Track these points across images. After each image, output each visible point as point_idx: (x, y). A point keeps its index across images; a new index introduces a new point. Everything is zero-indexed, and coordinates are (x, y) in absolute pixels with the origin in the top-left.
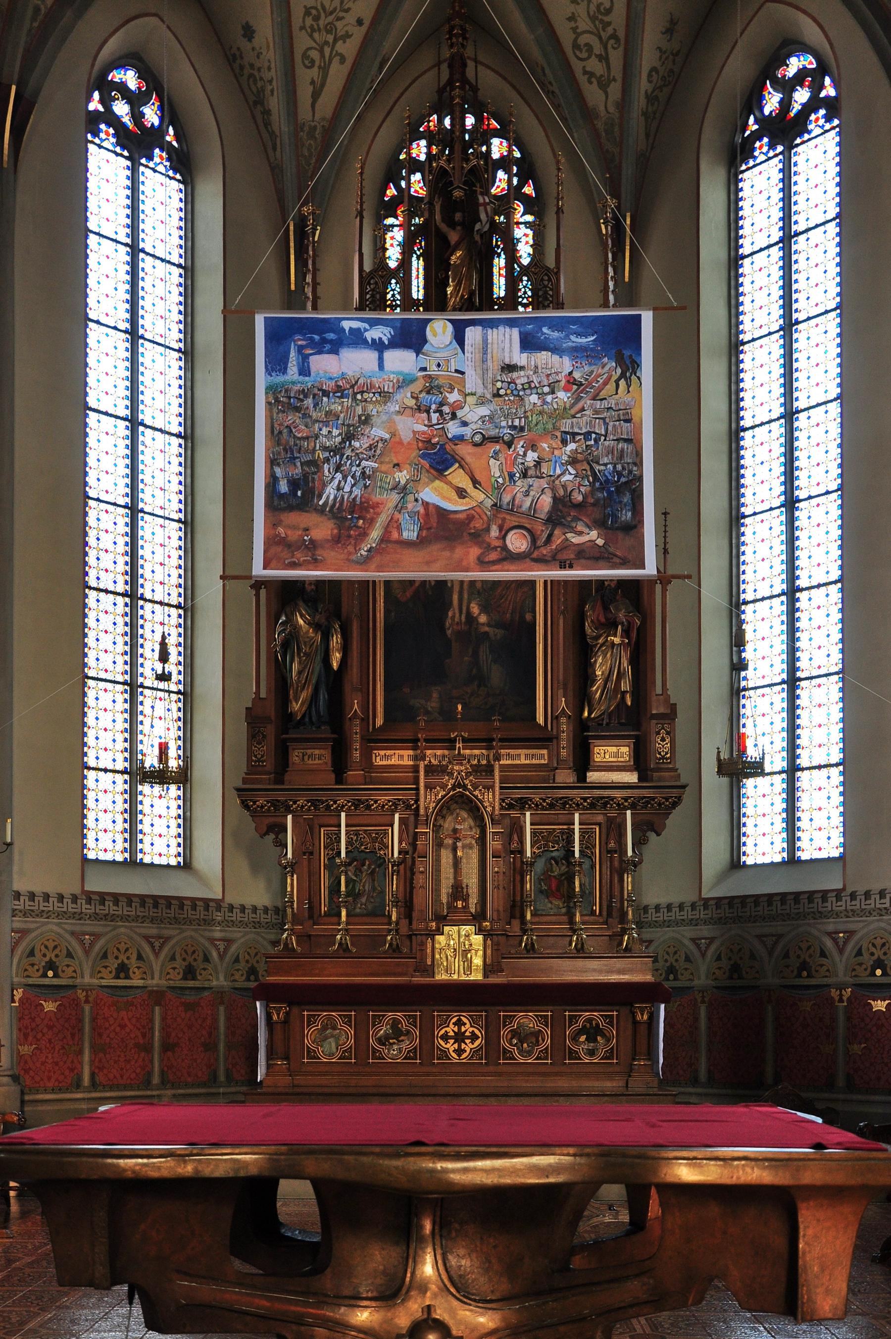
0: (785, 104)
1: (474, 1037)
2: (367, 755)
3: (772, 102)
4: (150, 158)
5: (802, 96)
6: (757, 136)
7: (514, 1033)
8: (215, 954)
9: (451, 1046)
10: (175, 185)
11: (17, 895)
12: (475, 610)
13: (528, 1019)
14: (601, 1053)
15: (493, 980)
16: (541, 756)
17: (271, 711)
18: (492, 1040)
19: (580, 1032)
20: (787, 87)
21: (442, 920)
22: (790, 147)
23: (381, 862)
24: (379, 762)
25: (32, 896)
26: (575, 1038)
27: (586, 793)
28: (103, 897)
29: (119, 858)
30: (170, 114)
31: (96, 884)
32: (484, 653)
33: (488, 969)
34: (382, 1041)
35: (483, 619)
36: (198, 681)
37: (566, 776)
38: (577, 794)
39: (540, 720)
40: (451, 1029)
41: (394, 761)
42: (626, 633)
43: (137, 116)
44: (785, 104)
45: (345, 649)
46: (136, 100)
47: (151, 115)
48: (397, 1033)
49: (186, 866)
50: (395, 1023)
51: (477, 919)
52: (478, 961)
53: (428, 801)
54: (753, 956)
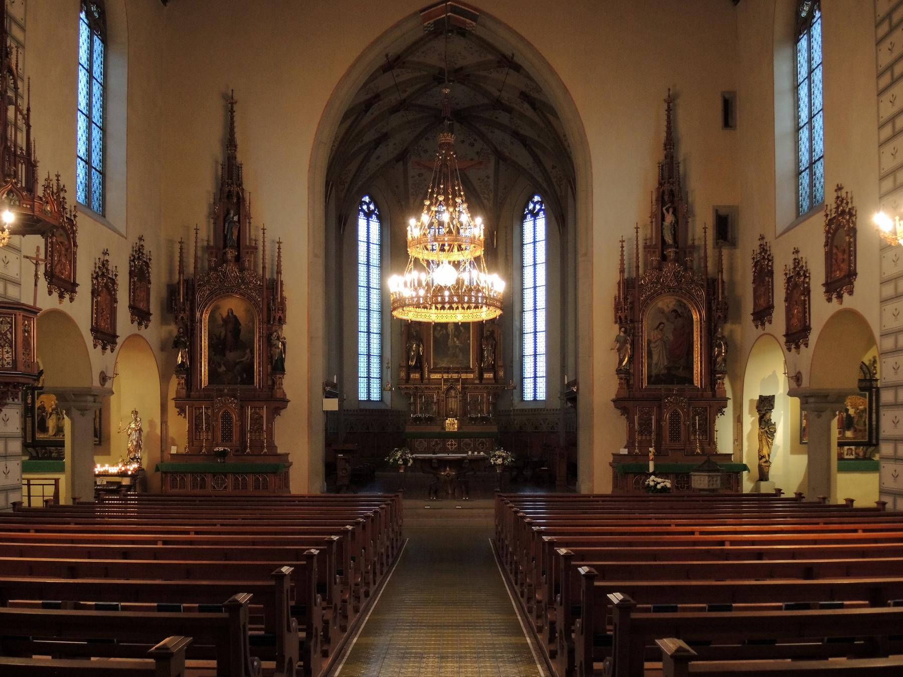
0: (534, 208)
1: (455, 445)
2: (429, 376)
3: (531, 206)
4: (372, 218)
5: (538, 207)
6: (527, 214)
7: (465, 444)
8: (389, 423)
9: (450, 447)
10: (378, 224)
11: (344, 410)
12: (455, 339)
13: (468, 440)
14: (485, 448)
15: (461, 431)
16: (471, 376)
17: (404, 364)
18: (459, 444)
19: (480, 443)
20: (535, 204)
21: (448, 416)
22: (535, 219)
23: (433, 402)
24: (432, 377)
25: (347, 410)
26: (479, 445)
27: (483, 386)
28: (363, 410)
29: (366, 399)
30: (376, 207)
31: (362, 407)
32: (457, 350)
33: (458, 428)
34: (433, 446)
35: (457, 342)
36: (384, 353)
37: (477, 382)
38: (480, 386)
39: (471, 367)
40: (450, 443)
41: (435, 377)
42: (492, 346)
43: (368, 208)
44: (534, 208)
45: (423, 349)
46: (368, 204)
47: (372, 207)
48: (437, 444)
49: (382, 400)
50: (436, 441)
51: (455, 416)
52: (456, 426)
53: (444, 387)
54: (525, 424)
